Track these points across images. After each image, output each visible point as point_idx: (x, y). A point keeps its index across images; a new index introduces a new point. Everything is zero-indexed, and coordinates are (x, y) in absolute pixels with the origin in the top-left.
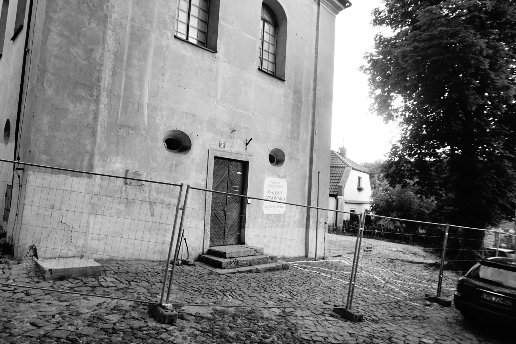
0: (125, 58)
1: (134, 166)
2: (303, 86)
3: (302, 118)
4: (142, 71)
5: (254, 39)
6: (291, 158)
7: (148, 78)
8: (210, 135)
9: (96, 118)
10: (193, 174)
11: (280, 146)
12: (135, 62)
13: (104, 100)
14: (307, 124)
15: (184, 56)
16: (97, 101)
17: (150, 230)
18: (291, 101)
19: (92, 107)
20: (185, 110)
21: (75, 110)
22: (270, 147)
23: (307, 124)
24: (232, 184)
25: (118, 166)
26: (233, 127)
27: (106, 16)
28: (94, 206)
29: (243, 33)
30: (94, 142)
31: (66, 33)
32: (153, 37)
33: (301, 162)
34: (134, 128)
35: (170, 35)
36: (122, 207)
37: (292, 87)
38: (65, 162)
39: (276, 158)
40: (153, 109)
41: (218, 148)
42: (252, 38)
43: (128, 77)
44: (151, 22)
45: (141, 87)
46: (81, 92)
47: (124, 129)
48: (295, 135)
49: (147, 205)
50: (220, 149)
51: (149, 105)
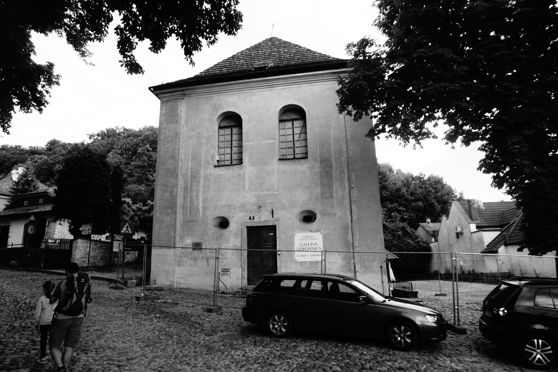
0: (189, 188)
1: (197, 241)
2: (333, 153)
3: (334, 179)
4: (198, 191)
5: (273, 141)
6: (324, 214)
7: (201, 194)
8: (242, 214)
9: (175, 221)
10: (232, 240)
11: (310, 207)
12: (194, 188)
13: (179, 211)
14: (342, 183)
15: (220, 175)
16: (175, 213)
17: (207, 274)
18: (318, 170)
19: (174, 216)
20: (224, 204)
21: (167, 219)
22: (298, 210)
23: (342, 183)
24: (266, 242)
25: (189, 241)
26: (260, 205)
27: (177, 174)
28: (179, 262)
29: (262, 142)
30: (175, 232)
31: (163, 188)
32: (202, 173)
33: (339, 214)
34: (195, 221)
35: (211, 167)
36: (192, 262)
37: (319, 159)
38: (164, 243)
39: (309, 218)
40: (205, 209)
41: (249, 221)
42: (271, 141)
43: (191, 197)
44: (201, 165)
45: (198, 199)
46: (169, 211)
47: (190, 223)
48: (327, 195)
49: (205, 260)
50: (251, 221)
51: (203, 207)
